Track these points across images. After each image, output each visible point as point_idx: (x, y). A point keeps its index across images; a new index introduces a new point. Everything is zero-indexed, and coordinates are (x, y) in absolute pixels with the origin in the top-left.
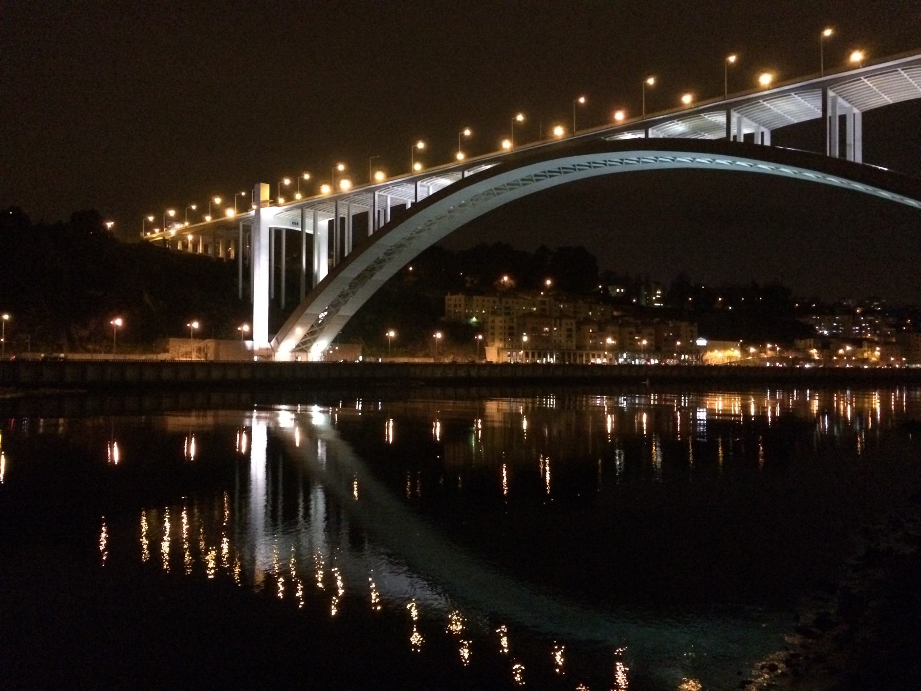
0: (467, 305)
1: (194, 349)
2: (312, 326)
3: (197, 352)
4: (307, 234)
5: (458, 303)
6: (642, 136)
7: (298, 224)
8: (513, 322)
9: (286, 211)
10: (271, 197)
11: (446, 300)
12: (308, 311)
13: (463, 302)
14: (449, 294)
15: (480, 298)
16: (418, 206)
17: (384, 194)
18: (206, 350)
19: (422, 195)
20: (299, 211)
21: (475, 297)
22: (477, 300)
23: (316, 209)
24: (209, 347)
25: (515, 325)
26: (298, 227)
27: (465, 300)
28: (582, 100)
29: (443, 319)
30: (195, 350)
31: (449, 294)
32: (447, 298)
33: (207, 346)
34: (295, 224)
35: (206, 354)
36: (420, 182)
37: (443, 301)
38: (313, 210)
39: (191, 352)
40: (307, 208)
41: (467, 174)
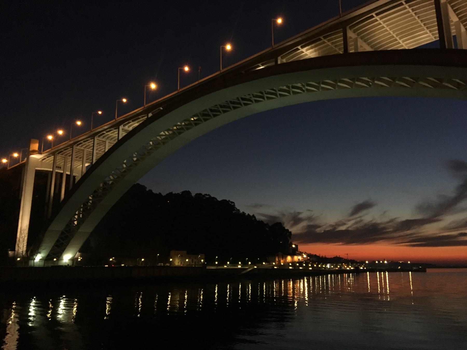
2: (58, 241)
4: (67, 175)
6: (273, 64)
7: (60, 168)
9: (48, 157)
10: (38, 149)
12: (50, 229)
16: (120, 143)
17: (104, 140)
19: (122, 134)
20: (53, 156)
23: (66, 155)
26: (60, 170)
28: (228, 47)
34: (58, 167)
36: (122, 126)
38: (63, 156)
40: (59, 153)
41: (150, 115)
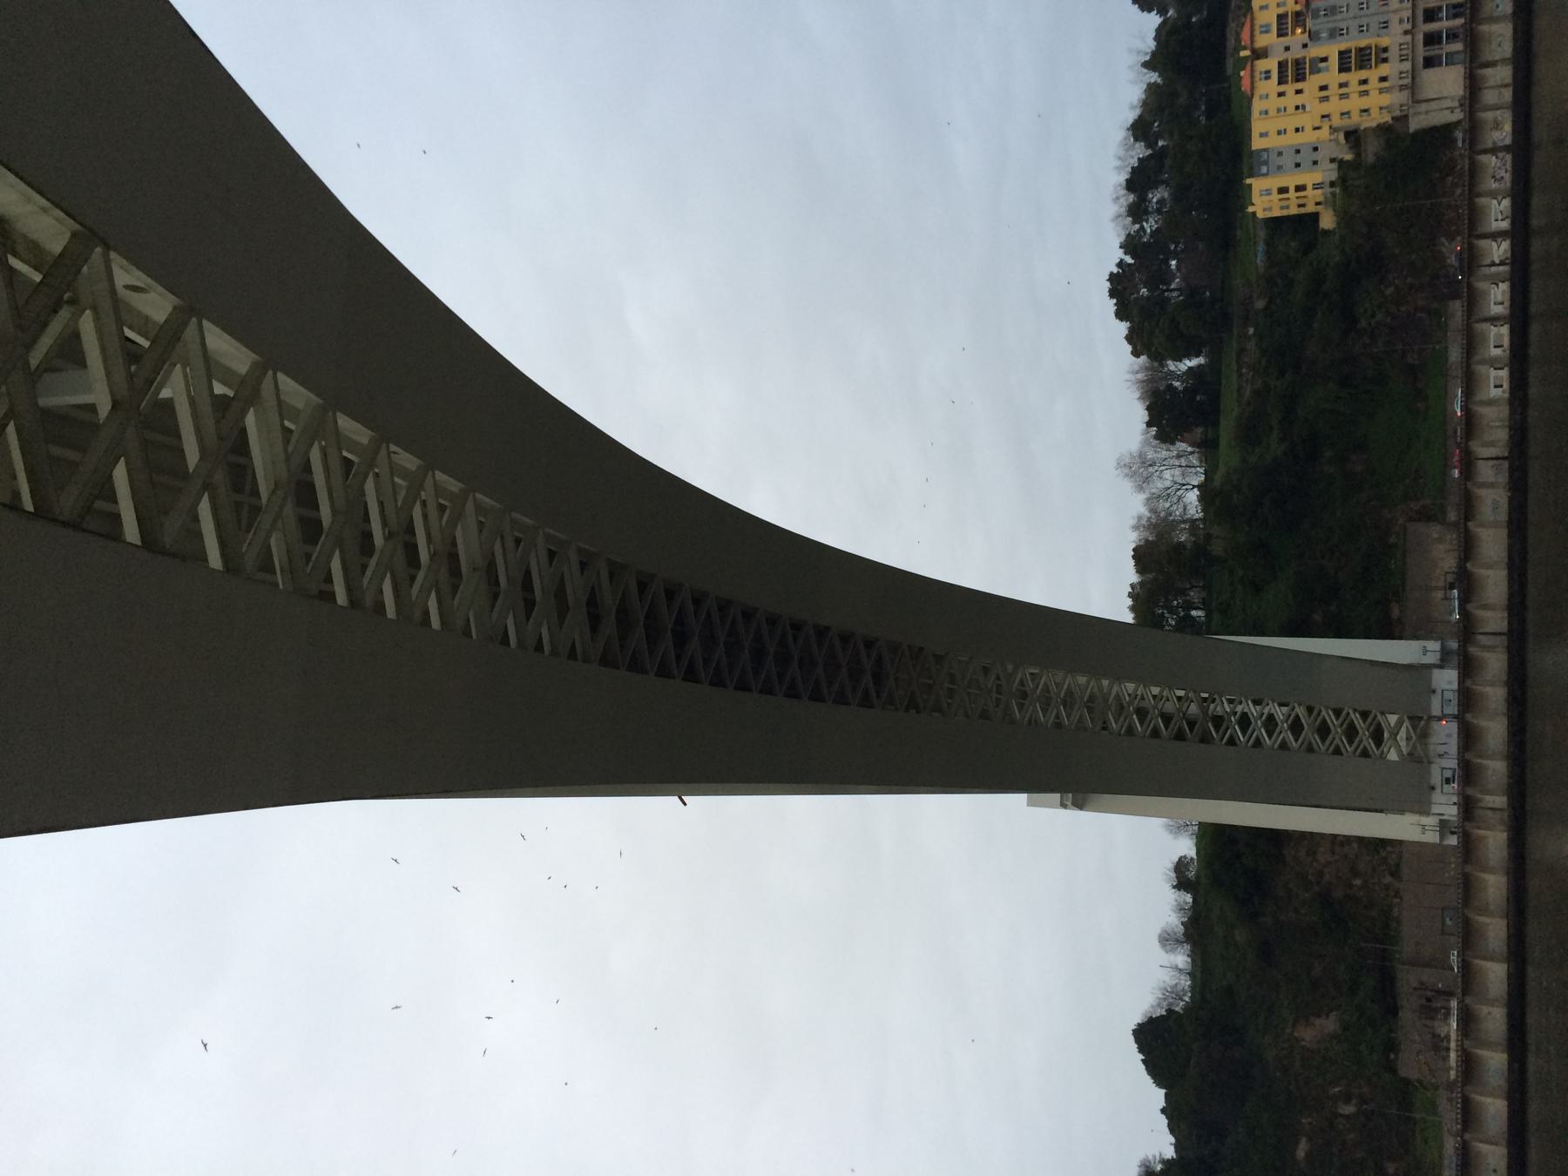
0: (1280, 168)
1: (1426, 1026)
3: (1432, 1018)
5: (1275, 196)
8: (1324, 60)
11: (1269, 215)
13: (1274, 183)
14: (1251, 209)
15: (1257, 126)
18: (1429, 994)
21: (1257, 143)
22: (1262, 135)
24: (1422, 983)
25: (1332, 50)
27: (1264, 175)
29: (1327, 221)
30: (1428, 1022)
31: (1251, 209)
32: (1260, 215)
33: (1415, 989)
35: (1439, 992)
37: (1275, 224)
39: (1434, 1035)
